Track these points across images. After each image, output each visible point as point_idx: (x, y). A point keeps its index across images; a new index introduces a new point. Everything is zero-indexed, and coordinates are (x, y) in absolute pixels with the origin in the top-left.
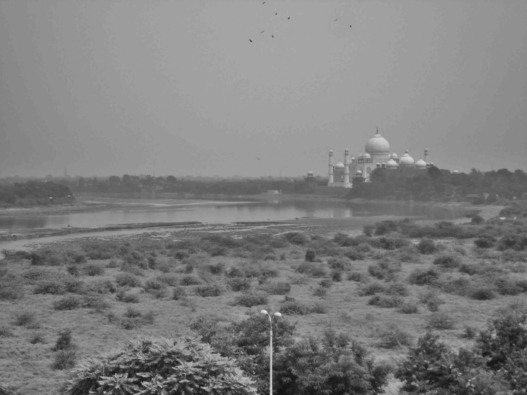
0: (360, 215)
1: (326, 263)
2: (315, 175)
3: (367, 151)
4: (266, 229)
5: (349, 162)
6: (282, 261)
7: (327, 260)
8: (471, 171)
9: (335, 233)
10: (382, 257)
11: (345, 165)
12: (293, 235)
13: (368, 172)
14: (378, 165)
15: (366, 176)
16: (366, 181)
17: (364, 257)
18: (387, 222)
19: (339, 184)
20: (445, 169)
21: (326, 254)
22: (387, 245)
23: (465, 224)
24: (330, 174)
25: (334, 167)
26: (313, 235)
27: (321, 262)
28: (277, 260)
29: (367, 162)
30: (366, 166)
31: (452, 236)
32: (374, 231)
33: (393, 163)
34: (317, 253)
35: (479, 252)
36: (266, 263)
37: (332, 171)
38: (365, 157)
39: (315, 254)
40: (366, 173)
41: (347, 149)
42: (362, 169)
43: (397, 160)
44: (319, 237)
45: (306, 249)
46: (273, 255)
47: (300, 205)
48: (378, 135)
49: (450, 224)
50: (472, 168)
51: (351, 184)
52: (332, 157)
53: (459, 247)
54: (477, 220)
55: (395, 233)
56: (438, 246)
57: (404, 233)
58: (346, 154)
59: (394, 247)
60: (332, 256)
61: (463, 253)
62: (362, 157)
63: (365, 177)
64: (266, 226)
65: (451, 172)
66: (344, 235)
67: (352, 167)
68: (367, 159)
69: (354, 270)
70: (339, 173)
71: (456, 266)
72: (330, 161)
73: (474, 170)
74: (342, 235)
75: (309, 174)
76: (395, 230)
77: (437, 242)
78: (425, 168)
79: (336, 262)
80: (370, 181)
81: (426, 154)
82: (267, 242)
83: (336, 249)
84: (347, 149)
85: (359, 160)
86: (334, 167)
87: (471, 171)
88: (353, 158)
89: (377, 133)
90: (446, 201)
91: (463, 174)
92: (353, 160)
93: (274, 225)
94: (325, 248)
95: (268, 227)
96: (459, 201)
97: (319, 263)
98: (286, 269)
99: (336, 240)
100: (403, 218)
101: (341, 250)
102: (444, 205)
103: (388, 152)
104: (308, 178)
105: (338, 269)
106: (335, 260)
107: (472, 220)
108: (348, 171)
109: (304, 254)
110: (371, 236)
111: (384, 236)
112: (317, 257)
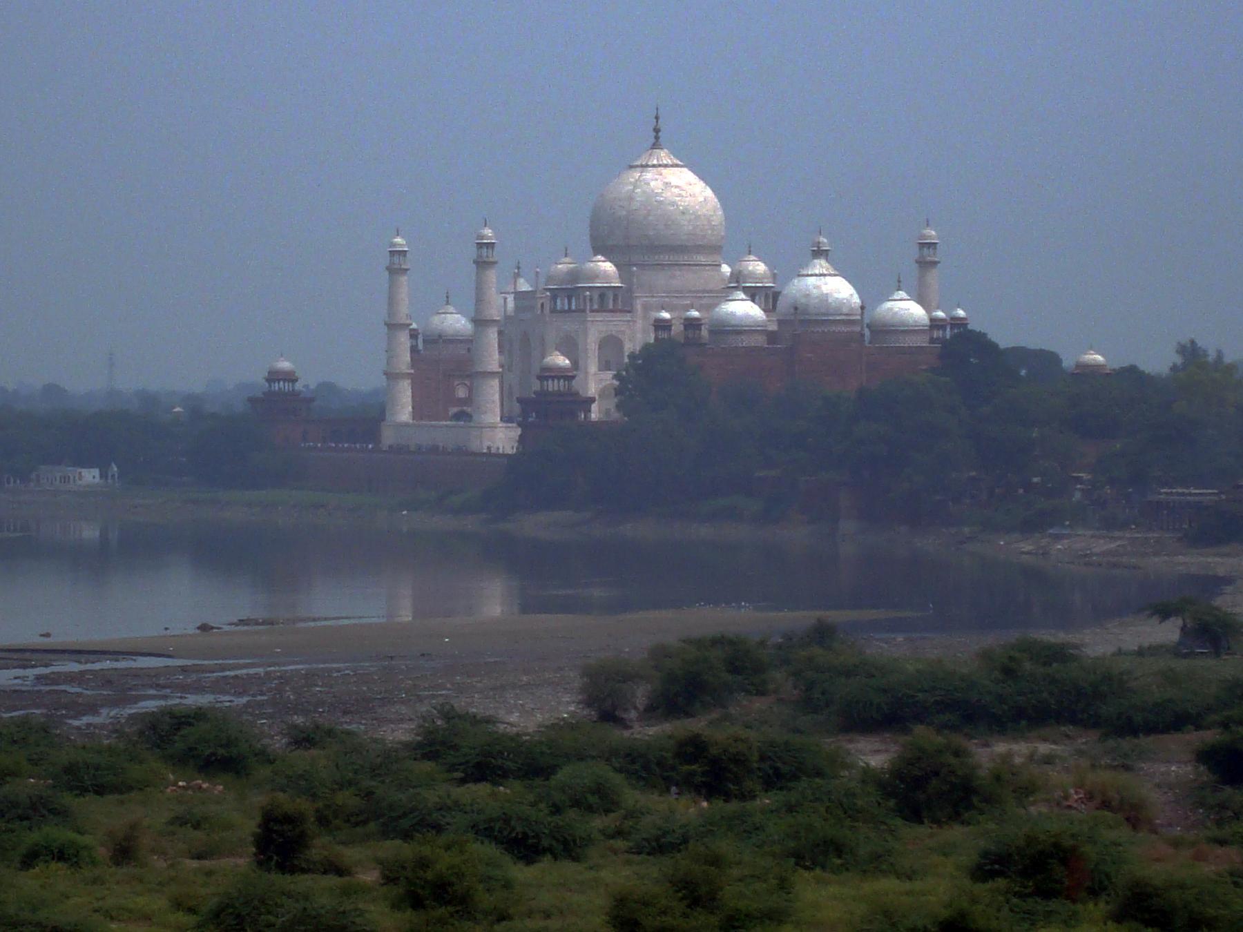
0: (566, 606)
1: (369, 877)
2: (308, 381)
3: (601, 247)
4: (27, 686)
5: (500, 304)
6: (124, 870)
7: (380, 862)
8: (1178, 360)
9: (423, 708)
10: (685, 841)
11: (480, 322)
12: (182, 720)
13: (605, 366)
14: (661, 325)
15: (596, 382)
16: (594, 416)
17: (588, 841)
18: (718, 642)
19: (443, 433)
20: (1033, 342)
21: (372, 826)
22: (712, 772)
23: (1141, 652)
24: (392, 376)
25: (414, 335)
26: (299, 720)
27: (339, 870)
28: (94, 863)
29: (602, 309)
30: (596, 329)
31: (1074, 721)
32: (641, 694)
33: (743, 309)
34: (323, 821)
35: (1222, 806)
36: (29, 882)
37: (406, 357)
38: (595, 276)
39: (311, 825)
40: (593, 368)
41: (488, 232)
42: (570, 346)
43: (765, 296)
44: (330, 733)
45: (259, 799)
46: (72, 835)
47: (218, 553)
48: (664, 156)
49: (1058, 654)
50: (1185, 341)
51: (516, 432)
52: (404, 279)
53: (1105, 776)
54: (1211, 633)
55: (759, 704)
56: (998, 778)
57: (808, 704)
58: (482, 264)
59: (748, 784)
60: (407, 836)
61: (1135, 815)
62: (574, 276)
63: (592, 390)
64: (31, 673)
65: (1068, 362)
66: (475, 720)
67: (520, 336)
68: (603, 293)
69: (530, 914)
70: (443, 369)
71: (1094, 893)
72: (392, 301)
73: (1191, 352)
74: (460, 717)
75: (274, 376)
76: (761, 693)
77: (990, 753)
78: (922, 341)
79: (429, 875)
80: (616, 415)
81: (925, 265)
82: (34, 762)
83: (431, 797)
84: (488, 232)
85: (555, 294)
86: (414, 335)
87: (1178, 360)
88: (524, 286)
89: (656, 145)
90: (1032, 525)
91: (1131, 373)
92: (519, 296)
93: (74, 667)
94: (369, 794)
95: (39, 678)
96: (1110, 524)
97: (332, 880)
98: (147, 918)
99: (432, 747)
100: (801, 618)
101: (456, 803)
102: (1031, 548)
103: (715, 249)
104: (269, 395)
105: (442, 911)
106: (423, 864)
107: (1183, 629)
108: (492, 359)
109: (249, 826)
110: (623, 724)
111: (697, 725)
112: (320, 846)
